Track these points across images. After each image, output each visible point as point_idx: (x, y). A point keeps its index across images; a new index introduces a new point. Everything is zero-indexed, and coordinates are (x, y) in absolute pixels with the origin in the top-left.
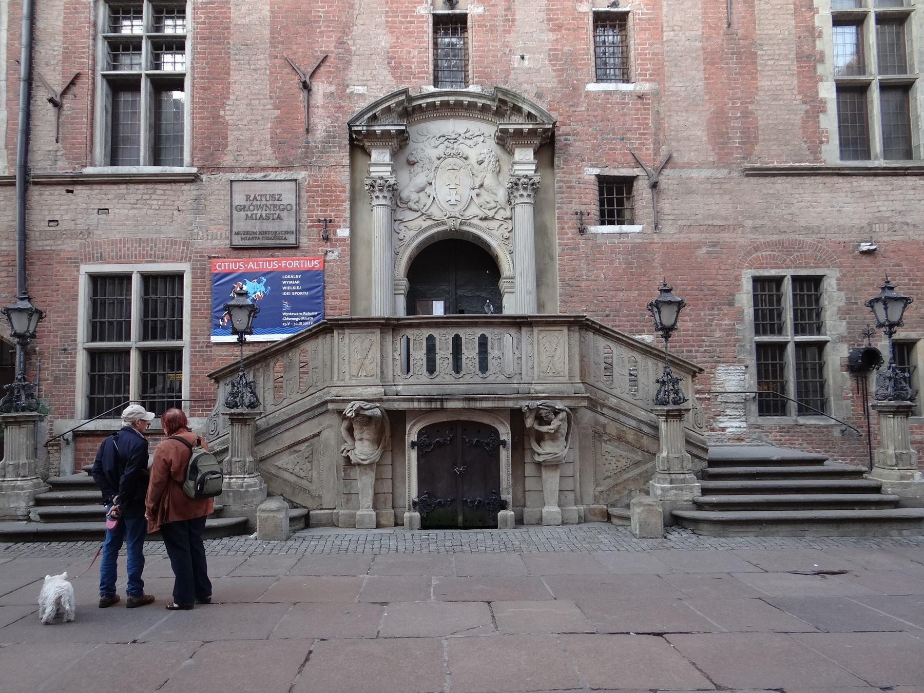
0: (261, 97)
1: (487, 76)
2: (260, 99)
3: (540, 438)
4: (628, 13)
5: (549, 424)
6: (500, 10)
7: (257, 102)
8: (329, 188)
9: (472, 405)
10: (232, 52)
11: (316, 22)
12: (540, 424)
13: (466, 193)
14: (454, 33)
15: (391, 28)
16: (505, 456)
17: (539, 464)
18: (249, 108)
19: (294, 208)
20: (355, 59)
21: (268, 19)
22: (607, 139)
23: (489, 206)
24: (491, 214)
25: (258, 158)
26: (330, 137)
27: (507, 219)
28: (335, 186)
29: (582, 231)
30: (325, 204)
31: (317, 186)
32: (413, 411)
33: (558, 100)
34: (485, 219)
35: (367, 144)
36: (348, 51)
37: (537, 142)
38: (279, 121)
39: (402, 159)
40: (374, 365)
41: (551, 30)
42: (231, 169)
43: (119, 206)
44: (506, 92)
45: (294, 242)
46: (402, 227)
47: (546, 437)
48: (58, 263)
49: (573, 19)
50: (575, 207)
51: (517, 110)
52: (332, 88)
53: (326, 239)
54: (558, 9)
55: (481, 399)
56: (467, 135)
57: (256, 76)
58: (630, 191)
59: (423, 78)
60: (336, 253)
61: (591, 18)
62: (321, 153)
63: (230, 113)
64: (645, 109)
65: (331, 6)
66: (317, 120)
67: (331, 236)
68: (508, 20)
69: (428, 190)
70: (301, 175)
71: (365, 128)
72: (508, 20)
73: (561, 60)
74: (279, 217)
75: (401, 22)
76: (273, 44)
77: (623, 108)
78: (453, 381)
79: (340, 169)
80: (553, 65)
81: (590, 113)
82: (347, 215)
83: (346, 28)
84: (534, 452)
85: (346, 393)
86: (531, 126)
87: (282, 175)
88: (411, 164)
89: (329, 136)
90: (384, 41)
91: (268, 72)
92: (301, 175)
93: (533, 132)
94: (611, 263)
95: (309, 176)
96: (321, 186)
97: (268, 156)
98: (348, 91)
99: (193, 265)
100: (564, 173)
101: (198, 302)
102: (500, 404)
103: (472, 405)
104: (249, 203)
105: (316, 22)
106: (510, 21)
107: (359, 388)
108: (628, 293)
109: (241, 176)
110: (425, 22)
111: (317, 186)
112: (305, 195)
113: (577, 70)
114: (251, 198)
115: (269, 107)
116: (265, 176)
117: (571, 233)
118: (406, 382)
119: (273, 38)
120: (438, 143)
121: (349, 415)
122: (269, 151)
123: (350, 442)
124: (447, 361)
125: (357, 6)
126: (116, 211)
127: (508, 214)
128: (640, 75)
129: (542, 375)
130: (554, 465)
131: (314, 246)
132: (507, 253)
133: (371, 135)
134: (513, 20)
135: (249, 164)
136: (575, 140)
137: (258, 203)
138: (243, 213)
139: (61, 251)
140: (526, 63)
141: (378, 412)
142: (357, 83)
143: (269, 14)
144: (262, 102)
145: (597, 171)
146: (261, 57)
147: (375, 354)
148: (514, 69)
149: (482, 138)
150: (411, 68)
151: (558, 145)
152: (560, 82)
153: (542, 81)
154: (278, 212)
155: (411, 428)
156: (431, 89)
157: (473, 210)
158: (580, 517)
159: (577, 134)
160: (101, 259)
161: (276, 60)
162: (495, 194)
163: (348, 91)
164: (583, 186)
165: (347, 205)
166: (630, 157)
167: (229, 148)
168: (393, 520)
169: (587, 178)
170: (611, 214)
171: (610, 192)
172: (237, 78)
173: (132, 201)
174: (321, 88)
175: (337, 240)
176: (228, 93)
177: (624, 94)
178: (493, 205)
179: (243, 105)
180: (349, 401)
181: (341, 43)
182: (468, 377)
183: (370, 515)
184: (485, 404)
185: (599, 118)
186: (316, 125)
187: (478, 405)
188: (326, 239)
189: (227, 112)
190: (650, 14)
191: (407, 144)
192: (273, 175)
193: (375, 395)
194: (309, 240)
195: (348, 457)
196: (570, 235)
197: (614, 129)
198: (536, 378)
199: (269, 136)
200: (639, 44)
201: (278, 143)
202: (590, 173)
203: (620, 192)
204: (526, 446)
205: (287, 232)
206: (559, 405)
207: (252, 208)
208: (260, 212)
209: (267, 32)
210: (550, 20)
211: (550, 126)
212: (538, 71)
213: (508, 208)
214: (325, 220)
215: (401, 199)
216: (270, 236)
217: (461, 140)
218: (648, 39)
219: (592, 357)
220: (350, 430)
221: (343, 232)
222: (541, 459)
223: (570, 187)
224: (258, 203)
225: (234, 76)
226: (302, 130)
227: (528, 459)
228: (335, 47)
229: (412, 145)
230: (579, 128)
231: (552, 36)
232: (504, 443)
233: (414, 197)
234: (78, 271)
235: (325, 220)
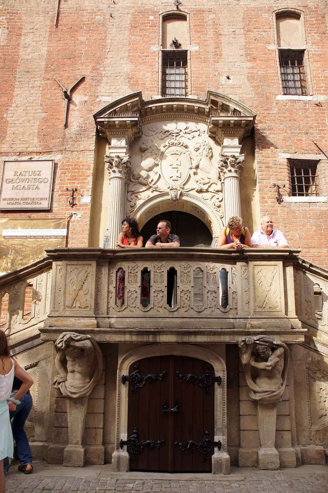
0: (34, 105)
1: (202, 90)
2: (33, 106)
3: (256, 375)
4: (305, 50)
5: (266, 360)
6: (211, 48)
7: (31, 108)
8: (77, 167)
9: (186, 339)
10: (17, 76)
11: (78, 57)
12: (256, 361)
13: (185, 172)
14: (178, 65)
15: (131, 59)
16: (220, 394)
17: (255, 403)
18: (24, 112)
19: (49, 180)
20: (105, 79)
21: (45, 56)
22: (295, 133)
23: (203, 181)
24: (205, 187)
25: (27, 145)
26: (82, 132)
27: (218, 191)
28: (83, 165)
29: (280, 200)
30: (74, 178)
31: (68, 165)
32: (125, 343)
33: (256, 106)
34: (200, 191)
35: (108, 134)
36: (100, 74)
37: (241, 132)
38: (45, 120)
39: (137, 148)
40: (88, 296)
41: (248, 61)
42: (7, 154)
44: (217, 95)
46: (133, 196)
47: (263, 374)
49: (264, 54)
50: (272, 182)
51: (225, 108)
52: (86, 98)
53: (73, 205)
54: (254, 48)
55: (196, 333)
56: (186, 131)
57: (32, 92)
58: (314, 172)
59: (154, 91)
60: (79, 215)
61: (277, 54)
62: (75, 141)
63: (11, 115)
64: (322, 113)
65: (90, 47)
66: (73, 119)
67: (76, 202)
68: (217, 54)
69: (155, 169)
70: (57, 157)
71: (107, 120)
72: (217, 54)
73: (257, 80)
74: (37, 188)
75: (139, 56)
76: (46, 71)
77: (305, 113)
78: (167, 314)
79: (88, 153)
80: (251, 83)
81: (281, 115)
82: (90, 186)
83: (99, 60)
84: (250, 390)
85: (59, 323)
86: (236, 119)
87: (44, 157)
88: (143, 151)
89: (80, 130)
90: (126, 67)
91: (41, 89)
92: (57, 157)
93: (238, 124)
94: (304, 225)
95: (63, 158)
96: (72, 165)
97: (35, 144)
98: (98, 100)
100: (263, 156)
102: (216, 339)
103: (186, 339)
104: (16, 177)
105: (78, 57)
106: (218, 55)
107: (72, 319)
108: (319, 250)
109: (12, 159)
110: (156, 56)
111: (68, 165)
112: (59, 171)
113: (269, 86)
114: (18, 174)
115: (39, 111)
116: (30, 159)
117: (271, 201)
118: (120, 314)
119: (47, 67)
120: (164, 136)
121: (60, 345)
122: (36, 140)
123: (62, 374)
124: (161, 294)
125: (108, 47)
127: (219, 187)
128: (316, 90)
129: (258, 310)
130: (270, 404)
131: (63, 209)
132: (219, 218)
133: (111, 126)
134: (221, 55)
135: (19, 150)
136: (270, 133)
137: (23, 177)
138: (10, 185)
140: (231, 81)
141: (88, 343)
142: (105, 94)
143: (46, 52)
144: (34, 108)
145: (289, 156)
146: (38, 79)
147: (90, 285)
148: (221, 85)
149: (198, 133)
150: (145, 84)
151: (257, 137)
152: (256, 94)
153: (243, 93)
154: (37, 184)
155: (123, 362)
156: (160, 97)
157: (191, 184)
158: (297, 459)
159: (272, 129)
161: (49, 82)
162: (209, 173)
163: (98, 100)
164: (278, 166)
165: (90, 179)
166: (313, 147)
167: (7, 139)
168: (102, 456)
169: (281, 160)
170: (300, 189)
171: (299, 173)
172: (18, 93)
174: (77, 97)
175: (80, 206)
176: (11, 103)
177: (305, 103)
178: (207, 181)
179: (20, 111)
180: (60, 331)
181: (95, 69)
182: (182, 311)
183: (78, 452)
184: (200, 339)
185: (288, 119)
186: (72, 123)
187: (193, 339)
188: (73, 205)
189: (9, 115)
190: (321, 51)
191: (141, 137)
192: (36, 158)
193: (88, 326)
194: (59, 205)
195: (59, 389)
196: (270, 203)
197: (299, 126)
198: (252, 312)
199: (37, 131)
200: (314, 70)
201: (43, 135)
202: (283, 157)
203: (306, 173)
204: (242, 383)
205: (42, 199)
206: (277, 340)
207: (18, 181)
208: (23, 184)
209: (43, 64)
210: (247, 55)
211: (252, 119)
212: (240, 87)
213: (219, 183)
214: (73, 190)
215: (133, 176)
216: (29, 201)
217: (182, 134)
218: (320, 67)
219: (303, 295)
220: (63, 363)
221: (87, 199)
222: (257, 397)
223: (268, 167)
224: (23, 177)
225: (17, 91)
226: (62, 126)
227: (243, 397)
228: (91, 72)
229: (144, 138)
230: (273, 125)
231: (249, 65)
232: (219, 380)
233: (143, 173)
235: (73, 190)
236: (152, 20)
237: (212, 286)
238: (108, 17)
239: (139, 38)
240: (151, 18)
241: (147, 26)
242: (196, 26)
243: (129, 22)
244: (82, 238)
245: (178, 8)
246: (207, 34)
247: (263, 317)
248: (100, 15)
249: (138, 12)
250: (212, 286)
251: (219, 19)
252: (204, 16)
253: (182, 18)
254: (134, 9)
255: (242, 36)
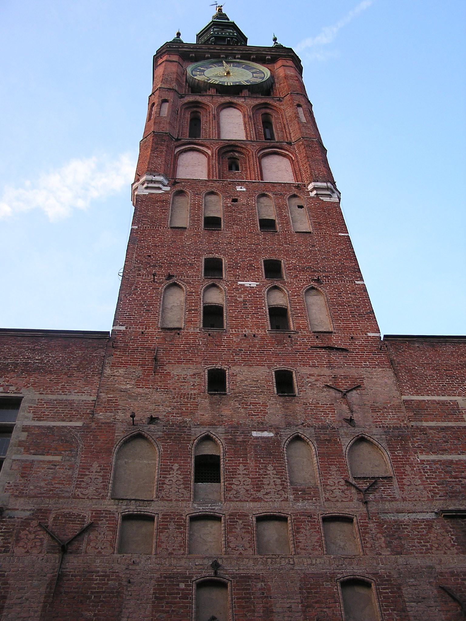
236: (183, 590)
238: (124, 583)
239: (165, 615)
240: (182, 586)
241: (176, 598)
242: (240, 598)
243: (152, 591)
245: (216, 573)
246: (254, 611)
248: (114, 580)
249: (165, 577)
251: (269, 590)
252: (249, 585)
253: (222, 585)
254: (159, 573)
255: (299, 614)
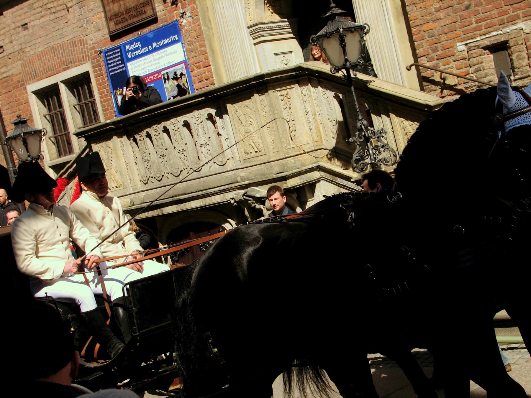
43: (32, 18)
45: (152, 13)
48: (14, 88)
99: (92, 63)
101: (105, 101)
126: (32, 23)
139: (13, 75)
160: (36, 77)
173: (39, 10)
216: (134, 13)
234: (26, 92)
237: (203, 139)
244: (200, 48)
247: (252, 165)
250: (203, 139)
